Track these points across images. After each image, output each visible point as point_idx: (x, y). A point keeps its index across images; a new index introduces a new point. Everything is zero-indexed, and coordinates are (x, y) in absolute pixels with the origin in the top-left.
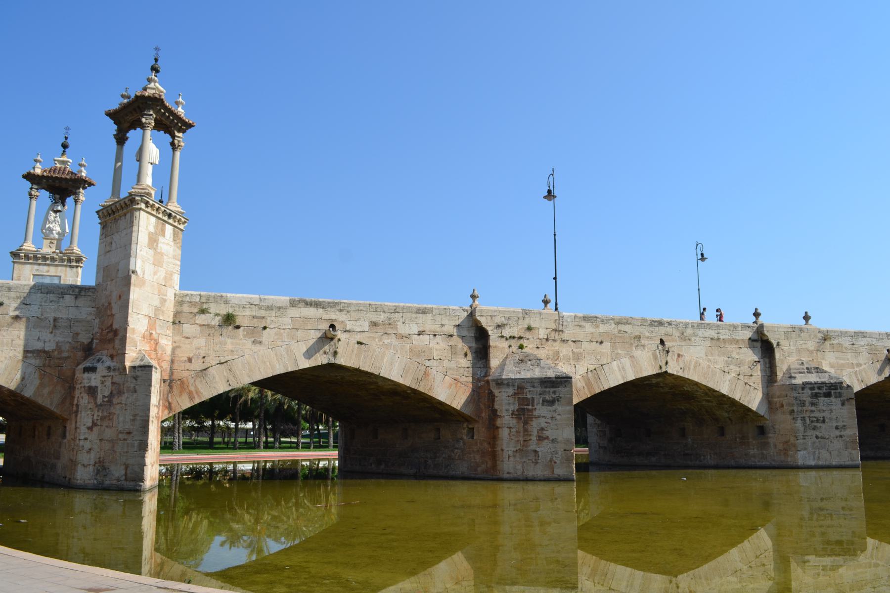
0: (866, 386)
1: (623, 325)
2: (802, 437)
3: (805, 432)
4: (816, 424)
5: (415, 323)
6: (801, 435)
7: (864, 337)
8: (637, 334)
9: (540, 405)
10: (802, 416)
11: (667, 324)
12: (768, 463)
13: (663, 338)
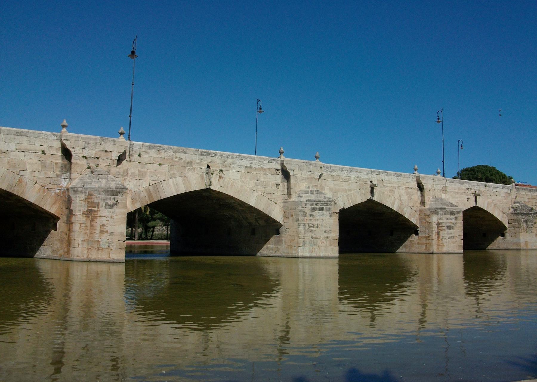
0: (353, 205)
1: (180, 153)
2: (302, 237)
3: (304, 234)
4: (312, 229)
5: (14, 142)
6: (302, 235)
7: (356, 172)
8: (189, 160)
9: (103, 208)
10: (304, 223)
11: (213, 154)
12: (280, 254)
13: (209, 165)
